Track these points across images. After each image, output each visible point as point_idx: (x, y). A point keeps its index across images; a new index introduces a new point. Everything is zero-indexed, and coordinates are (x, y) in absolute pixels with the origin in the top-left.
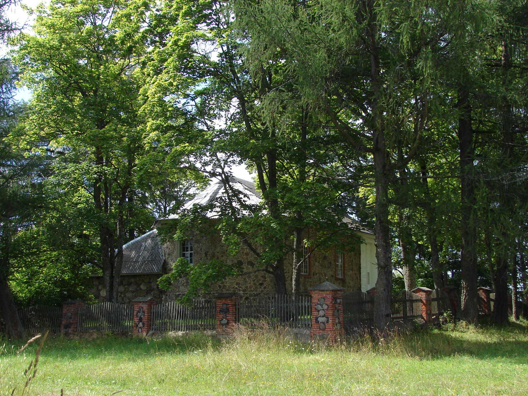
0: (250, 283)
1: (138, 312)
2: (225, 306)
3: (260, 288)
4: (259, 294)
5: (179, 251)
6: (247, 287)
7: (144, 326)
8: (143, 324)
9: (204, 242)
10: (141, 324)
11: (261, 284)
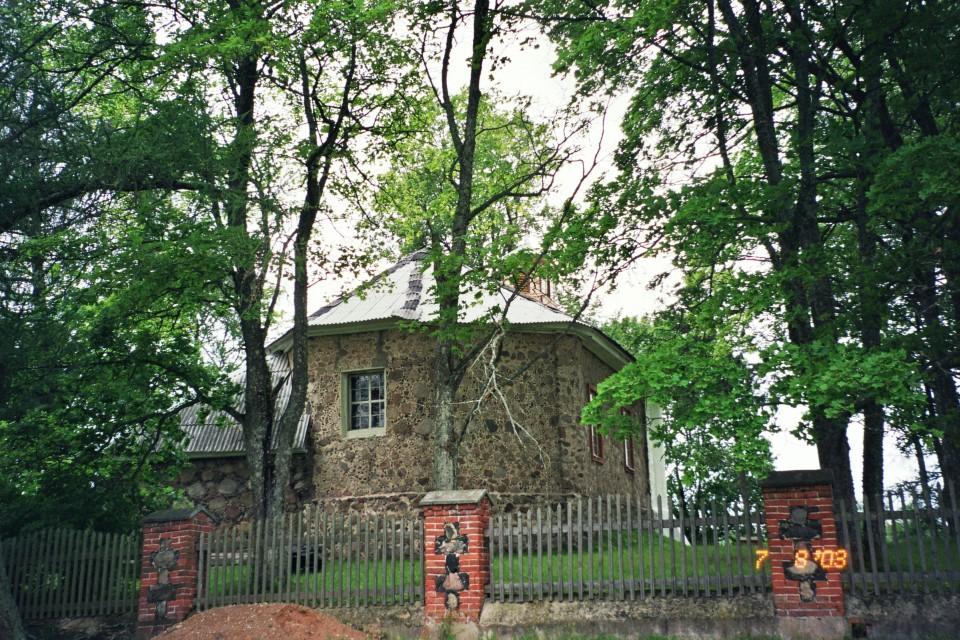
0: (513, 472)
1: (442, 538)
2: (801, 515)
3: (534, 483)
4: (533, 497)
5: (345, 398)
6: (506, 481)
7: (466, 586)
8: (465, 578)
9: (415, 377)
10: (453, 581)
11: (535, 475)
